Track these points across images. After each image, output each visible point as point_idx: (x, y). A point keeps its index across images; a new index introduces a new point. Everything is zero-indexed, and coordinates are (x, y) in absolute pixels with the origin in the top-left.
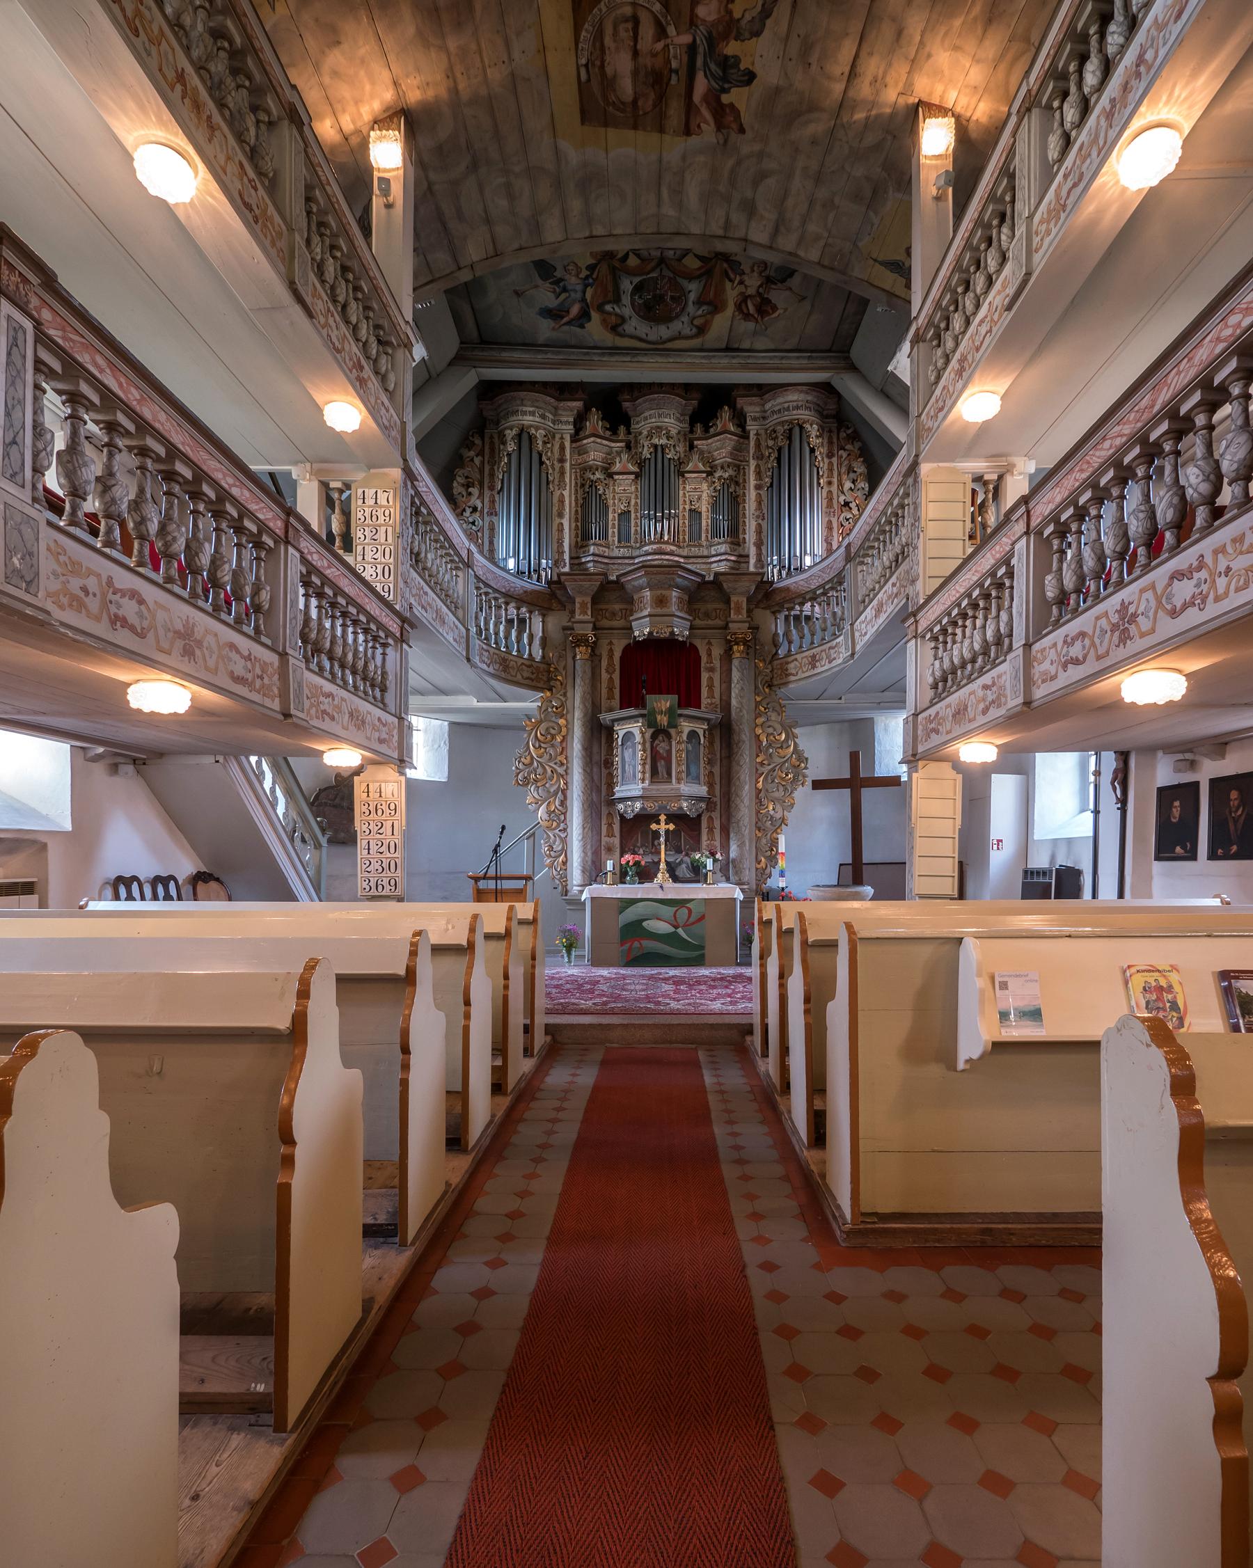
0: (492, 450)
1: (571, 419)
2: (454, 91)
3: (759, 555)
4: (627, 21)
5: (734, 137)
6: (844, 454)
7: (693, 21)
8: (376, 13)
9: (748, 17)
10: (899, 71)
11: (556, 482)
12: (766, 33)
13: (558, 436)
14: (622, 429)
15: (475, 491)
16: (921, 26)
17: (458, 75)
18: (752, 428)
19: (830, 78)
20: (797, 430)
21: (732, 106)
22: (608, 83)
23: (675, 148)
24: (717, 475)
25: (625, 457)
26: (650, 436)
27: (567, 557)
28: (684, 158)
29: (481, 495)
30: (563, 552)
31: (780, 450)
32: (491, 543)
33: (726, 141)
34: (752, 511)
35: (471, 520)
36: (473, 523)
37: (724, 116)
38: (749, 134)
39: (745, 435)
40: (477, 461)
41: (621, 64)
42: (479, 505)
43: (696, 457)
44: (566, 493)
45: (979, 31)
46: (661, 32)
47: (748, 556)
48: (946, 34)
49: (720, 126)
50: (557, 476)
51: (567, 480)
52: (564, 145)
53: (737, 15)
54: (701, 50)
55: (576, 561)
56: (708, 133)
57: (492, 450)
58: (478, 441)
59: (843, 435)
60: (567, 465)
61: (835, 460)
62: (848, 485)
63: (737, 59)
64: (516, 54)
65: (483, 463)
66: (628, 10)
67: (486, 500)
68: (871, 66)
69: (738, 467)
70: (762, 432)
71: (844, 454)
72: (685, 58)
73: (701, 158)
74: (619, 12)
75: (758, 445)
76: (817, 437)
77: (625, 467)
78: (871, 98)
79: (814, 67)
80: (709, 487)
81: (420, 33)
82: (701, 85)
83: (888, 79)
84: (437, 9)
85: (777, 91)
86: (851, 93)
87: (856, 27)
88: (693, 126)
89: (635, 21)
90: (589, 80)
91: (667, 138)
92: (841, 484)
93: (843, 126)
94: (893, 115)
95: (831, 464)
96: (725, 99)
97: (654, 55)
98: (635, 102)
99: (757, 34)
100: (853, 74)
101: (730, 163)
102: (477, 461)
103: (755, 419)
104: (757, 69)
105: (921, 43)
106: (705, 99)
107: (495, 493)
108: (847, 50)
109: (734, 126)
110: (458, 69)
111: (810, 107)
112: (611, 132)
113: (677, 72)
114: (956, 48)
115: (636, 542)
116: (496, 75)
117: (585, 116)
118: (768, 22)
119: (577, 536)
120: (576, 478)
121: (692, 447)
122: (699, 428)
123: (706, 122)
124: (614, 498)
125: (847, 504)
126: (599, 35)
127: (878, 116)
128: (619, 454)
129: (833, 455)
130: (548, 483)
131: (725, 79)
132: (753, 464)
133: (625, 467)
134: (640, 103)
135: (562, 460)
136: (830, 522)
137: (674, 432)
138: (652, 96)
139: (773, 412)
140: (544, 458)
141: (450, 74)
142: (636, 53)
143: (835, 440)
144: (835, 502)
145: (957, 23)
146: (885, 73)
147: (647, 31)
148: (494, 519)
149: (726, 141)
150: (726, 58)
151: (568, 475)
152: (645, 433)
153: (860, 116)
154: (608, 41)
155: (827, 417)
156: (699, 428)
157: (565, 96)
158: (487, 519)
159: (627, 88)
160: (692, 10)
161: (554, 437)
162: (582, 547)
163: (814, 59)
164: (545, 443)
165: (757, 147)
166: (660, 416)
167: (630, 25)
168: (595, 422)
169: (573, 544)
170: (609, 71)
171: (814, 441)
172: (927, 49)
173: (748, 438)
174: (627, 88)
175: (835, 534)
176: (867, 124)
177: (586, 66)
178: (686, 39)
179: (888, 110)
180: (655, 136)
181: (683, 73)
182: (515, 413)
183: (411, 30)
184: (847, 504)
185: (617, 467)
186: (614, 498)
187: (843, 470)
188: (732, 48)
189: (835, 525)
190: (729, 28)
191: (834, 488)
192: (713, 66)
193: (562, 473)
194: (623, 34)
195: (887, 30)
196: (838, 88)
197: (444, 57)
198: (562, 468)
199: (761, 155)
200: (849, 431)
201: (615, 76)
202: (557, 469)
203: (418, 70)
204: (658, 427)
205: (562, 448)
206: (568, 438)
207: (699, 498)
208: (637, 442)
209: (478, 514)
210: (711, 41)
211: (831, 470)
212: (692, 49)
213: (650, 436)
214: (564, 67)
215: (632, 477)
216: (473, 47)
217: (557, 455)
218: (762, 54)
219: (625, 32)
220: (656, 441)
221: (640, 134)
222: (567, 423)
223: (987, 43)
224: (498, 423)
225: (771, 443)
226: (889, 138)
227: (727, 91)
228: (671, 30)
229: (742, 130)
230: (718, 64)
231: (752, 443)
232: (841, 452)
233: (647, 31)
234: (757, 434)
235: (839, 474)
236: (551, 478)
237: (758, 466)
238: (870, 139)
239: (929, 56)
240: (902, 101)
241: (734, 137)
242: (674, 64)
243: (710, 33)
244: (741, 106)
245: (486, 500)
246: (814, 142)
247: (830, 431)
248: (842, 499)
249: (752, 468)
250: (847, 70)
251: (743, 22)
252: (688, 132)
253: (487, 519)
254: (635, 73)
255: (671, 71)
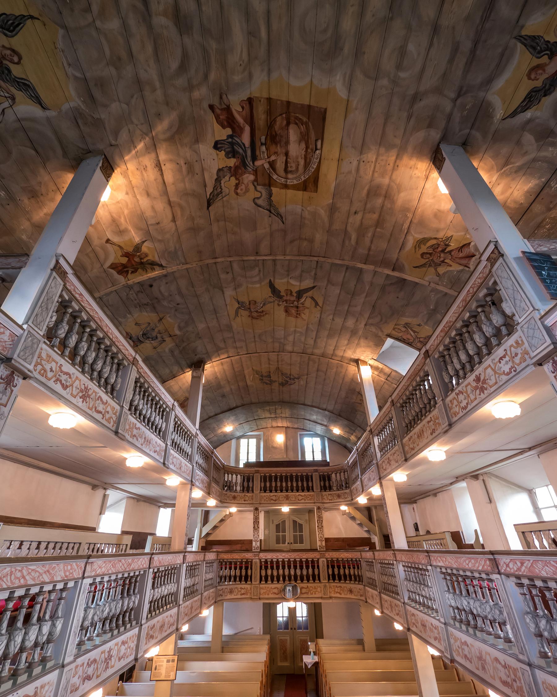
2: (399, 157)
4: (291, 171)
5: (216, 102)
7: (255, 172)
8: (413, 209)
9: (227, 178)
10: (136, 180)
12: (215, 172)
16: (141, 202)
17: (392, 165)
19: (171, 160)
21: (224, 127)
22: (304, 138)
23: (257, 87)
28: (251, 76)
33: (221, 98)
37: (229, 121)
38: (205, 105)
41: (295, 149)
45: (114, 215)
46: (272, 165)
48: (127, 205)
49: (228, 109)
52: (343, 93)
53: (233, 179)
54: (249, 159)
56: (235, 101)
63: (227, 156)
64: (355, 163)
66: (290, 176)
68: (152, 174)
72: (258, 153)
73: (237, 78)
74: (295, 176)
78: (141, 159)
79: (183, 164)
81: (399, 192)
82: (246, 139)
83: (138, 173)
84: (385, 197)
85: (197, 141)
86: (153, 155)
87: (171, 189)
88: (247, 107)
89: (286, 170)
90: (316, 140)
91: (265, 95)
93: (147, 134)
94: (122, 157)
96: (229, 131)
97: (276, 153)
98: (288, 124)
99: (219, 170)
100: (158, 165)
101: (212, 76)
104: (214, 152)
105: (135, 196)
106: (242, 129)
108: (169, 177)
109: (218, 111)
110: (390, 168)
111: (175, 137)
112: (306, 102)
113: (262, 144)
114: (118, 202)
116: (371, 156)
117: (323, 115)
118: (215, 177)
123: (238, 112)
126: (307, 165)
127: (130, 151)
131: (232, 144)
134: (285, 122)
138: (277, 127)
141: (396, 167)
142: (287, 154)
145: (126, 212)
146: (142, 175)
147: (280, 165)
149: (221, 98)
150: (234, 157)
153: (140, 146)
154: (302, 162)
157: (334, 132)
159: (293, 134)
160: (256, 176)
163: (184, 168)
165: (196, 94)
167: (289, 169)
170: (303, 145)
172: (130, 195)
174: (293, 134)
176: (132, 144)
177: (316, 149)
178: (258, 163)
179: (126, 158)
180: (274, 95)
181: (258, 144)
183: (402, 195)
188: (232, 162)
190: (235, 172)
192: (241, 151)
194: (294, 165)
195: (154, 192)
196: (163, 157)
197: (394, 177)
199: (191, 88)
201: (300, 142)
203: (411, 177)
210: (244, 164)
212: (254, 158)
214: (330, 149)
216: (376, 175)
218: (214, 161)
219: (292, 166)
221: (284, 99)
223: (107, 214)
226: (113, 142)
227: (229, 137)
228: (267, 166)
229: (211, 107)
230: (238, 152)
233: (280, 165)
238: (124, 135)
239: (127, 194)
240: (124, 167)
241: (216, 102)
242: (264, 148)
243: (245, 168)
244: (217, 127)
246: (159, 115)
250: (163, 168)
251: (229, 175)
252: (250, 101)
254: (287, 143)
255: (265, 144)
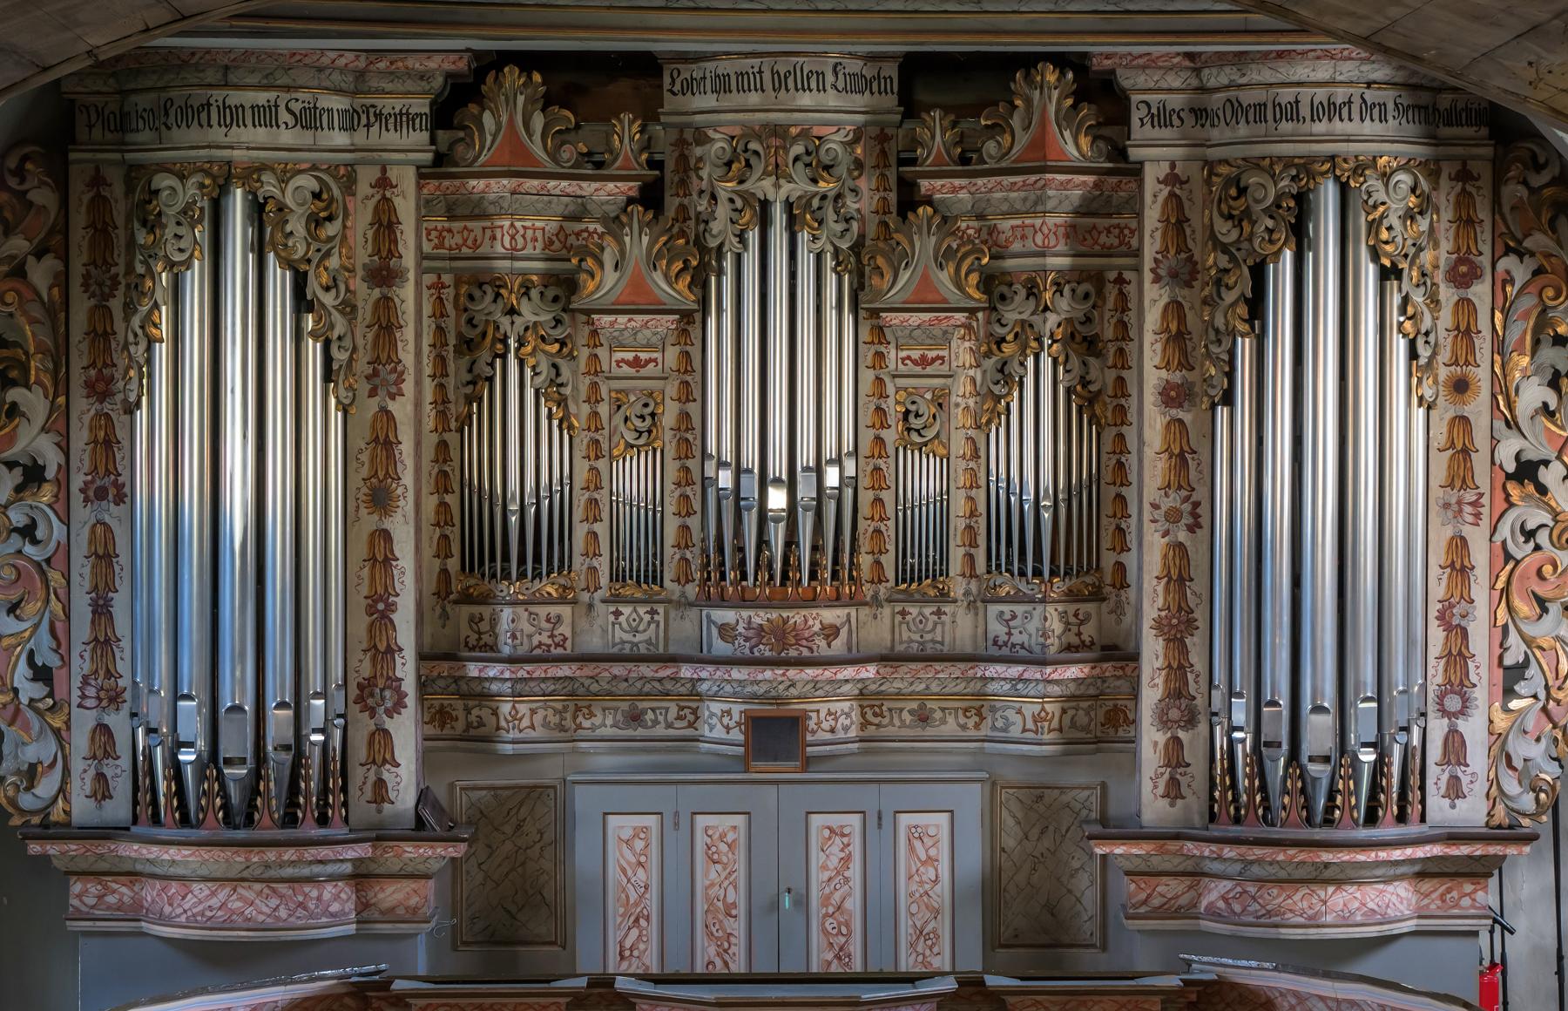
0: (101, 232)
1: (421, 106)
3: (1177, 670)
6: (1520, 272)
11: (362, 366)
13: (366, 177)
14: (626, 134)
15: (33, 401)
18: (1157, 154)
20: (1328, 194)
24: (1011, 316)
25: (638, 243)
26: (738, 161)
27: (406, 669)
29: (59, 423)
30: (392, 651)
31: (1258, 274)
32: (101, 610)
34: (1151, 491)
35: (17, 517)
36: (28, 532)
39: (1121, 165)
40: (40, 274)
42: (52, 459)
43: (925, 245)
44: (402, 409)
47: (1135, 657)
50: (364, 337)
51: (407, 356)
55: (444, 667)
57: (101, 232)
58: (43, 196)
59: (1513, 192)
60: (406, 295)
61: (1480, 292)
62: (1533, 394)
65: (62, 280)
67: (80, 438)
69: (1097, 278)
70: (1196, 173)
71: (1520, 272)
75: (1176, 223)
76: (1409, 216)
77: (638, 284)
80: (980, 357)
92: (1504, 391)
95: (1465, 305)
102: (40, 274)
103: (1161, 117)
107: (113, 407)
115: (684, 578)
119: (443, 551)
120: (439, 313)
121: (909, 200)
122: (936, 135)
124: (594, 398)
125: (1527, 471)
128: (614, 224)
129: (1474, 275)
130: (328, 376)
132: (1153, 301)
133: (638, 284)
135: (383, 275)
136: (1459, 544)
137: (835, 144)
139: (1237, 110)
140: (313, 288)
143: (1483, 213)
144: (1480, 461)
148: (112, 514)
151: (409, 333)
152: (719, 145)
155: (1451, 118)
156: (936, 135)
158: (82, 514)
161: (349, 183)
162: (466, 598)
164: (315, 222)
166: (780, 82)
168: (513, 111)
169: (431, 585)
171: (1398, 235)
173: (1136, 171)
175: (1480, 591)
182: (196, 113)
184: (1527, 471)
185: (605, 283)
186: (594, 398)
187: (1521, 330)
189: (1480, 555)
191: (1478, 407)
193: (386, 327)
198: (386, 305)
200: (1538, 180)
202: (365, 313)
204: (778, 131)
205: (385, 224)
206: (405, 179)
207: (940, 401)
208: (686, 167)
209: (47, 494)
211: (1465, 333)
213: (738, 161)
215: (667, 322)
217: (363, 255)
220: (764, 187)
222: (404, 119)
224: (121, 123)
225: (1223, 228)
231: (1152, 215)
232: (1507, 263)
234: (1172, 179)
235: (1499, 346)
236: (340, 356)
237: (1175, 308)
245: (80, 438)
247: (1464, 175)
248: (1507, 455)
249: (1152, 317)
253: (82, 514)
